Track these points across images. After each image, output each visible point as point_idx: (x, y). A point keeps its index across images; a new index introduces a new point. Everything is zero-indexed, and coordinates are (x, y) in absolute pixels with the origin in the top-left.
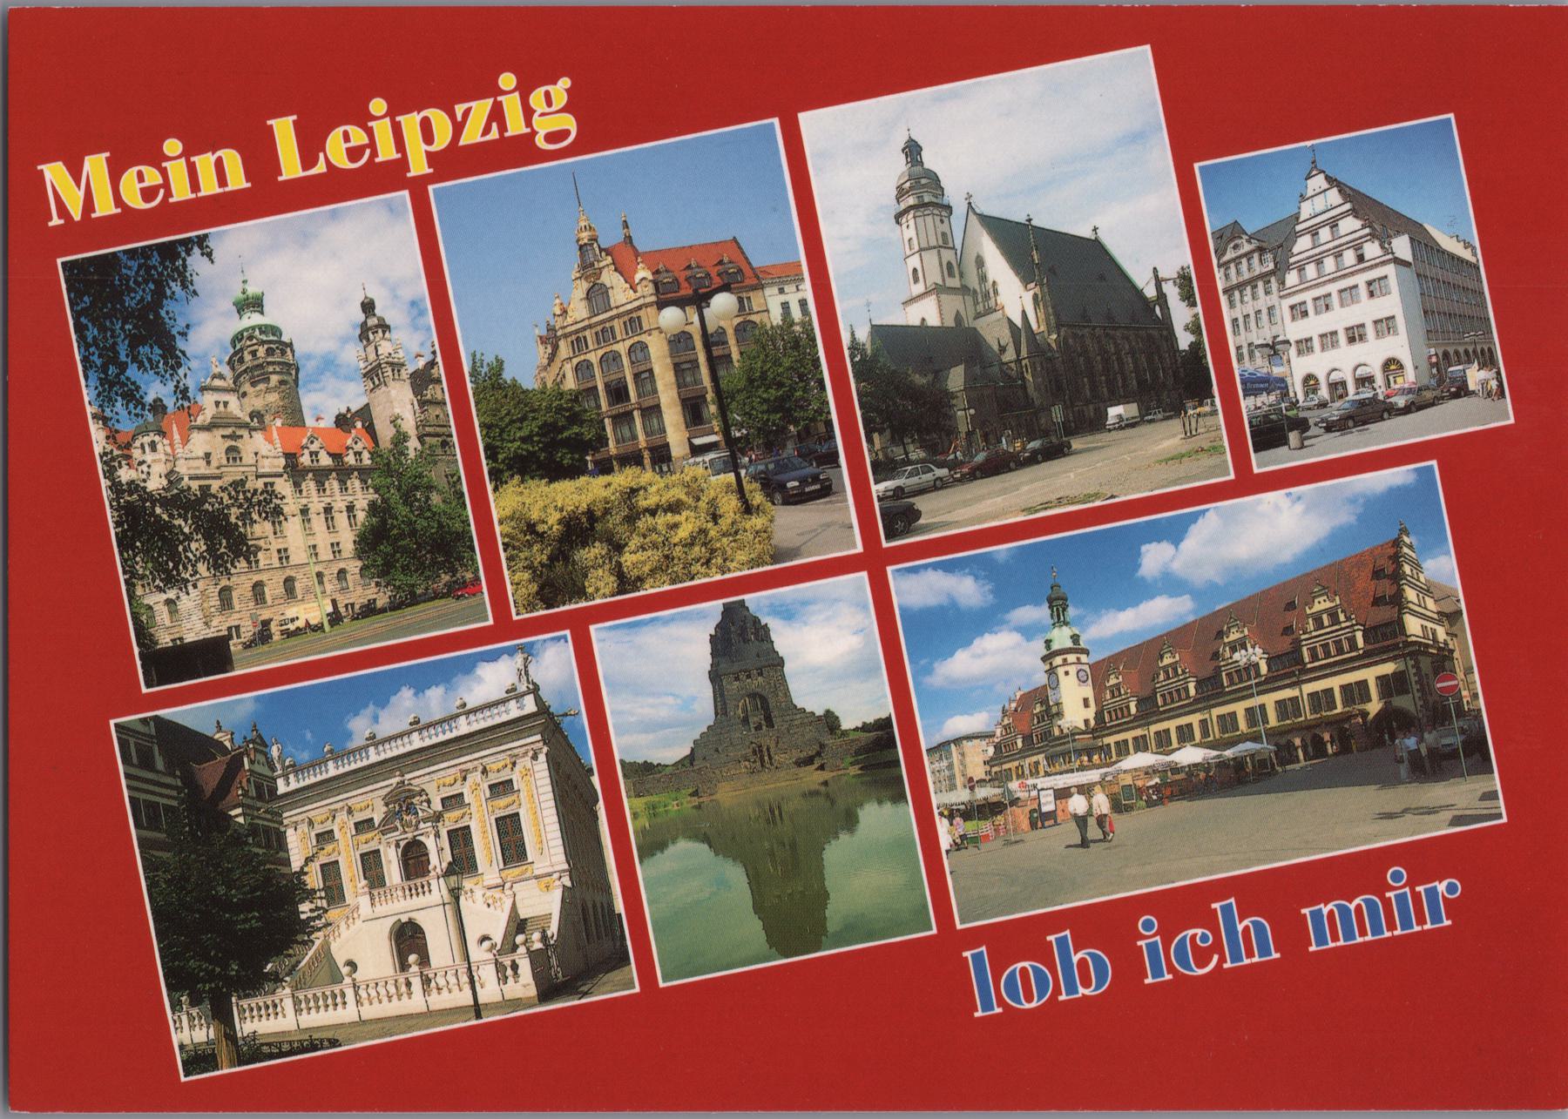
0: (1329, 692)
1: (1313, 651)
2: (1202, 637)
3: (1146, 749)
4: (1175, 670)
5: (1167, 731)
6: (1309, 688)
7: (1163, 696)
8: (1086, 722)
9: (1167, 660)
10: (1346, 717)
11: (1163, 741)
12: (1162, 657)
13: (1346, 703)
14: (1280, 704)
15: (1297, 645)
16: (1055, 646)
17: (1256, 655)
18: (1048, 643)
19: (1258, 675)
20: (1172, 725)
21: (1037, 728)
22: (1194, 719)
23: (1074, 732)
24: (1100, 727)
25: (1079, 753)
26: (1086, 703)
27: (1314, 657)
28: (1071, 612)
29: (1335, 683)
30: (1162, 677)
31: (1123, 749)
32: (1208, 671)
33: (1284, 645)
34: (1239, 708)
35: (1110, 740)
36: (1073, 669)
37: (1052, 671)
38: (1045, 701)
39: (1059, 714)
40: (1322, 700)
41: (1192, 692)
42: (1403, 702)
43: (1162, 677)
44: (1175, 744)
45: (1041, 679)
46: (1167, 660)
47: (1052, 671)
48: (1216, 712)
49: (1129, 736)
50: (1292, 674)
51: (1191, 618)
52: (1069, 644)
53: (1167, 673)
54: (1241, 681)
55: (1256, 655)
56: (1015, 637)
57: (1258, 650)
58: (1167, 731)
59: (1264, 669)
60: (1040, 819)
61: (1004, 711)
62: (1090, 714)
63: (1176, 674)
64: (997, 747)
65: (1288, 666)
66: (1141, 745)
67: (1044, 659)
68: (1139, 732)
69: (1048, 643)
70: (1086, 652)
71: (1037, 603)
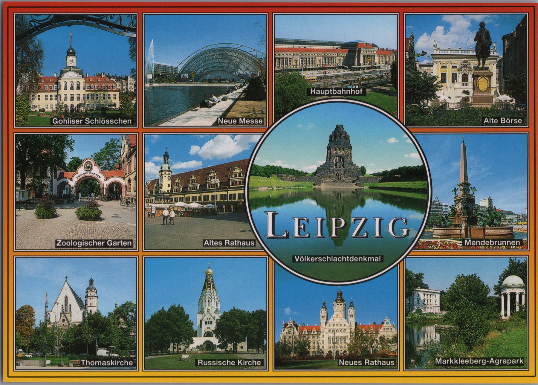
0: (235, 195)
1: (233, 183)
2: (203, 174)
3: (182, 201)
5: (189, 197)
6: (230, 192)
8: (168, 191)
9: (193, 178)
11: (188, 200)
13: (239, 198)
14: (221, 195)
16: (163, 169)
17: (218, 181)
19: (217, 186)
20: (191, 196)
22: (197, 195)
23: (165, 193)
24: (171, 193)
25: (164, 199)
27: (233, 185)
28: (169, 160)
31: (176, 200)
33: (226, 179)
34: (210, 194)
36: (167, 176)
37: (161, 176)
38: (158, 183)
39: (161, 188)
40: (233, 196)
41: (198, 188)
44: (191, 201)
46: (193, 178)
47: (161, 176)
48: (204, 194)
49: (179, 196)
52: (167, 169)
57: (218, 180)
58: (189, 197)
59: (219, 185)
62: (169, 189)
65: (225, 185)
66: (181, 200)
67: (160, 172)
69: (162, 168)
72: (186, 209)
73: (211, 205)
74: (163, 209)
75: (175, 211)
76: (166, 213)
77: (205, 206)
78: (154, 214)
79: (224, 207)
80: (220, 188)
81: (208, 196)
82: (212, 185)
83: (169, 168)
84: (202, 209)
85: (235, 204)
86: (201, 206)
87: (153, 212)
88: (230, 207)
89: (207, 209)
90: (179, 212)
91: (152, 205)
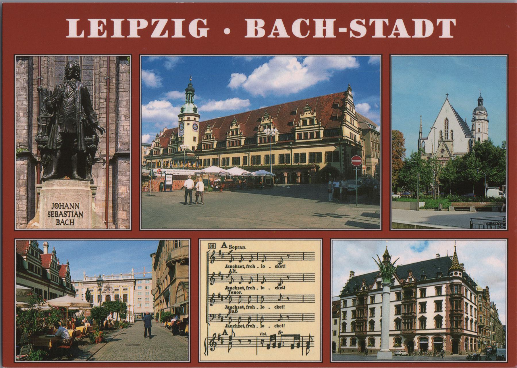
0: (304, 155)
2: (251, 120)
4: (237, 132)
5: (228, 159)
7: (229, 142)
9: (234, 127)
10: (309, 167)
11: (226, 162)
12: (232, 125)
14: (281, 156)
15: (294, 130)
16: (185, 111)
17: (275, 132)
18: (182, 109)
19: (274, 141)
20: (231, 156)
21: (170, 146)
23: (187, 151)
24: (198, 151)
25: (187, 161)
26: (195, 139)
27: (300, 138)
28: (195, 97)
29: (307, 151)
30: (230, 134)
31: (207, 163)
32: (252, 135)
33: (288, 130)
34: (262, 154)
35: (202, 158)
36: (191, 123)
37: (182, 122)
38: (176, 135)
42: (336, 165)
43: (230, 134)
45: (177, 125)
46: (234, 127)
47: (182, 122)
49: (211, 157)
50: (288, 144)
51: (248, 110)
52: (192, 111)
53: (233, 132)
54: (265, 142)
55: (275, 132)
56: (168, 104)
57: (276, 130)
58: (228, 159)
59: (277, 139)
60: (164, 187)
61: (157, 136)
62: (196, 144)
63: (237, 134)
65: (287, 139)
66: (215, 163)
67: (180, 116)
68: (215, 157)
69: (182, 109)
70: (199, 117)
71: (180, 91)
72: (222, 177)
73: (264, 172)
74: (185, 178)
75: (205, 182)
76: (189, 184)
77: (254, 174)
78: (170, 186)
79: (286, 174)
80: (279, 144)
81: (259, 157)
82: (265, 138)
83: (195, 109)
84: (250, 178)
85: (305, 170)
86: (248, 172)
87: (167, 183)
88: (295, 176)
89: (257, 179)
90: (211, 183)
91: (168, 171)
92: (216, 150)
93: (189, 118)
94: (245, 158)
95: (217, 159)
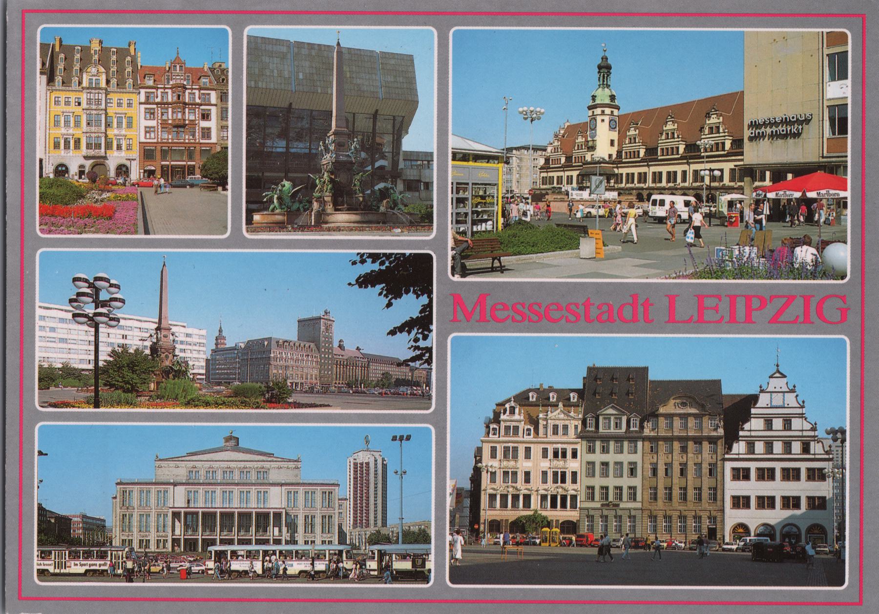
7: (662, 149)
8: (610, 156)
9: (670, 126)
16: (598, 101)
24: (618, 161)
26: (612, 143)
30: (663, 137)
36: (607, 119)
37: (593, 118)
43: (663, 137)
52: (607, 101)
61: (556, 136)
62: (614, 151)
63: (674, 138)
64: (547, 160)
70: (618, 108)
83: (613, 98)
92: (643, 161)
93: (603, 112)
94: (684, 173)
95: (645, 173)
